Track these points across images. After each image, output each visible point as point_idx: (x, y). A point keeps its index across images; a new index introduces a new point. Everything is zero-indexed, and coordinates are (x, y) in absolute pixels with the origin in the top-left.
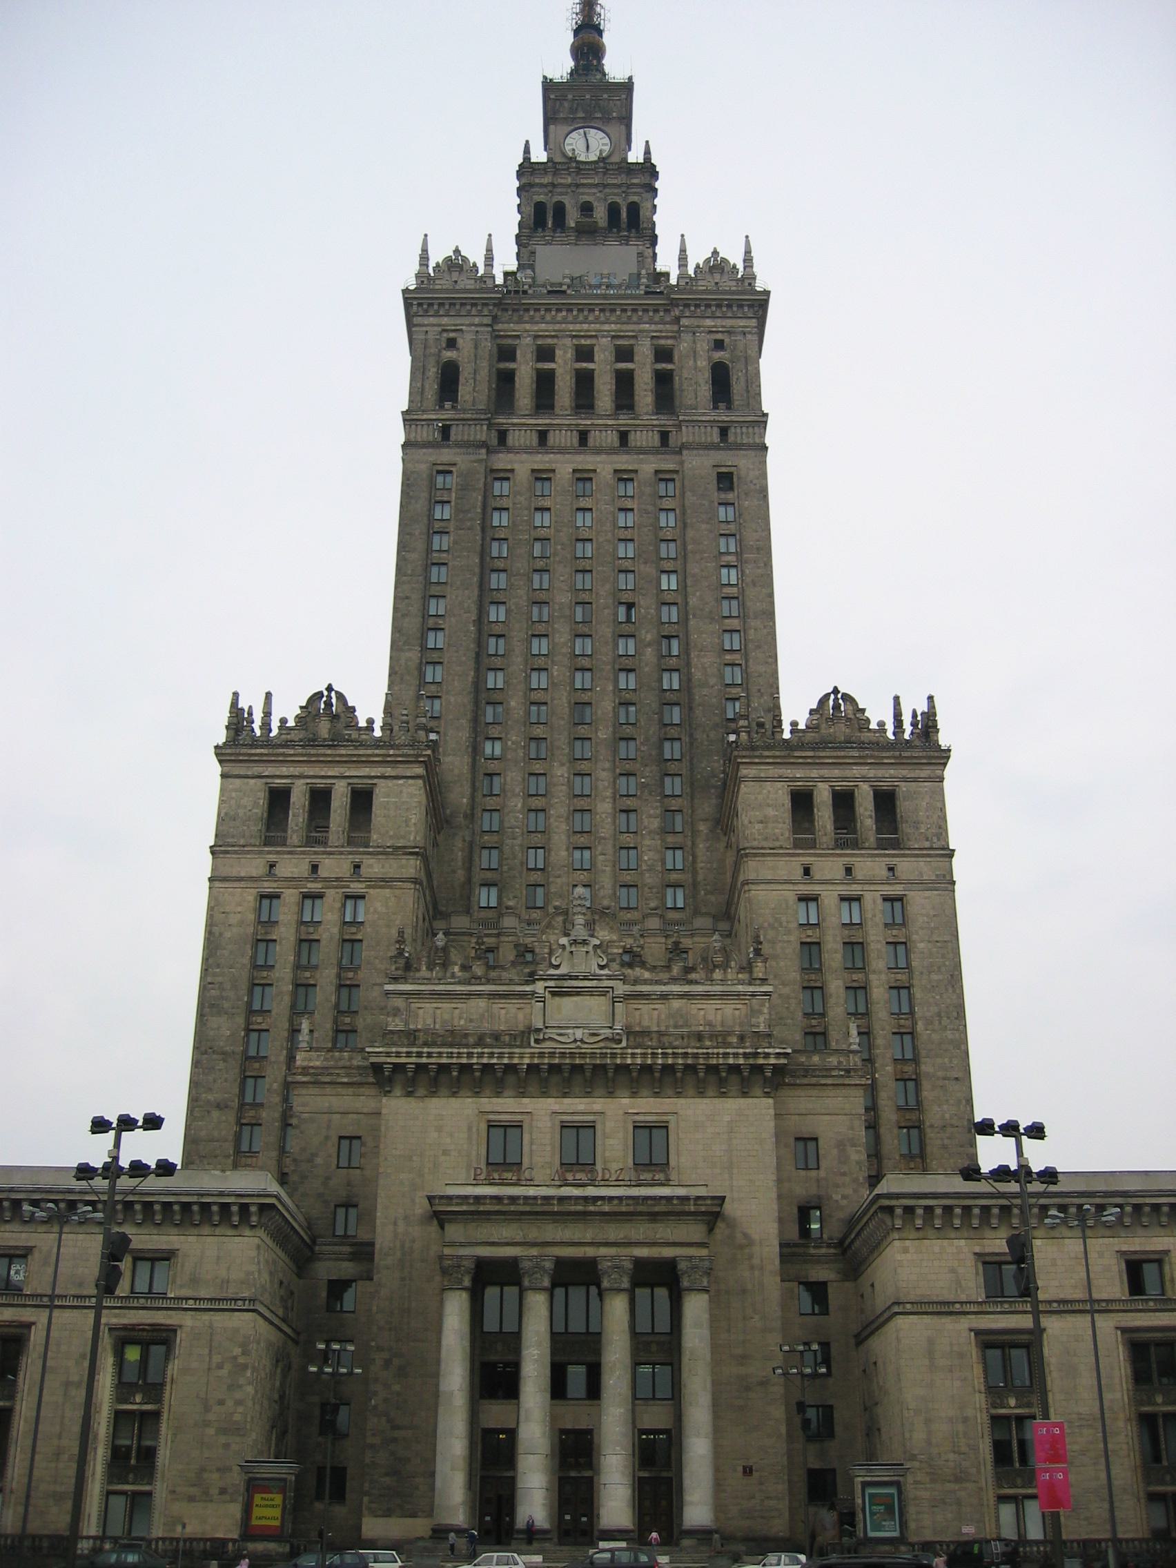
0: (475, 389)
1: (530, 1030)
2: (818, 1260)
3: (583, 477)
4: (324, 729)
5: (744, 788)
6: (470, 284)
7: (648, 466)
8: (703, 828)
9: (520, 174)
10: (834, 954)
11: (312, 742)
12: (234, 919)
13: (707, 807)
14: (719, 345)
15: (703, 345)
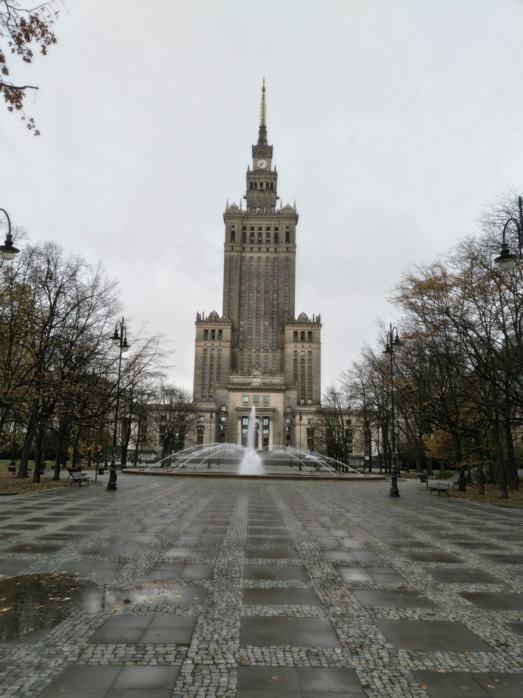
0: (238, 237)
2: (289, 415)
4: (214, 319)
6: (237, 212)
7: (272, 256)
8: (280, 332)
9: (247, 174)
11: (211, 321)
12: (200, 353)
13: (280, 328)
15: (284, 228)
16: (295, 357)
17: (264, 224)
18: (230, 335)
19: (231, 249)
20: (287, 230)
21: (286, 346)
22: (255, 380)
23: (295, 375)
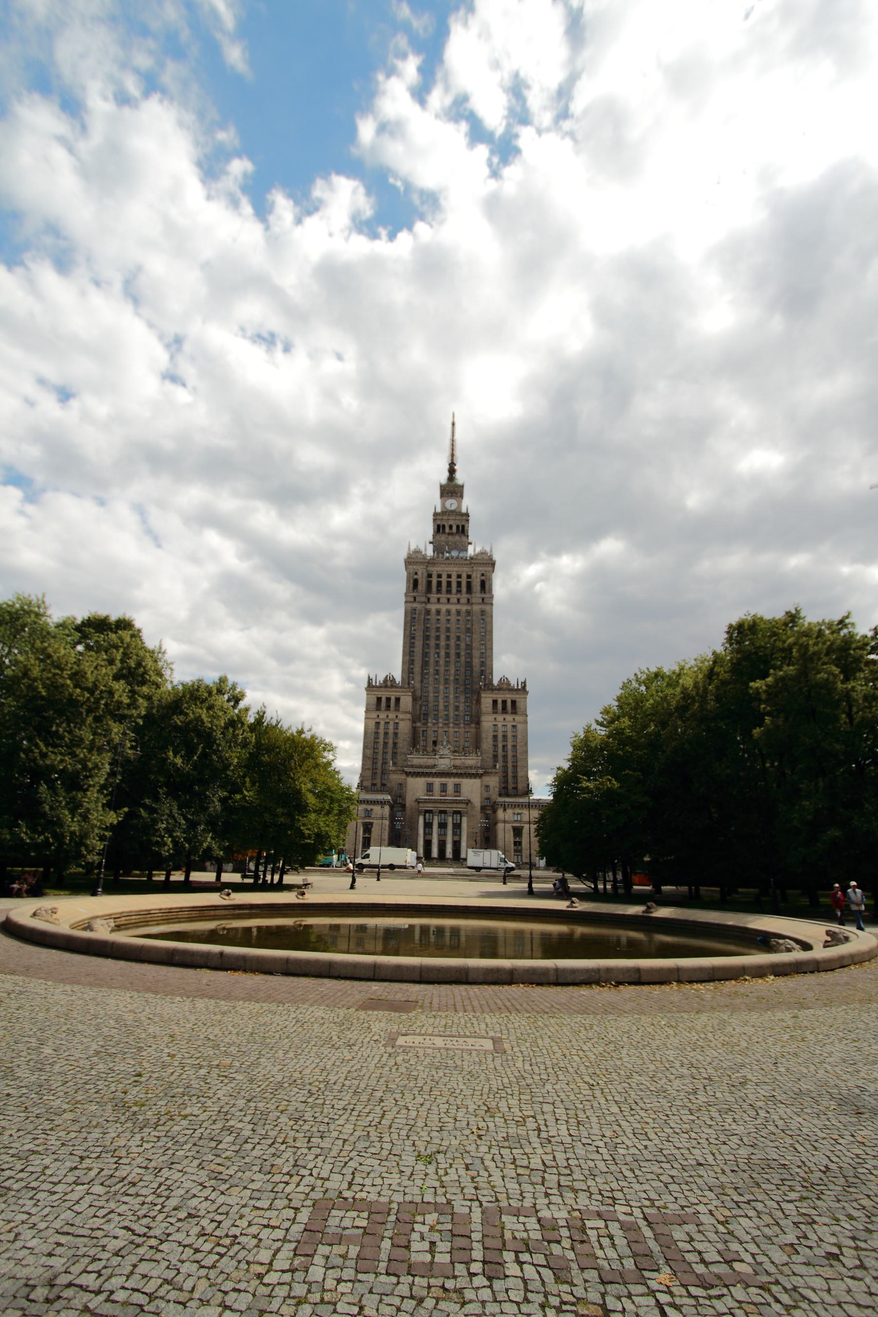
0: (422, 586)
3: (449, 612)
4: (389, 683)
5: (483, 700)
6: (420, 556)
7: (464, 608)
10: (500, 738)
11: (386, 686)
13: (475, 697)
14: (483, 575)
15: (479, 575)
16: (495, 734)
18: (410, 705)
19: (412, 600)
20: (483, 578)
21: (483, 718)
22: (442, 761)
23: (495, 757)
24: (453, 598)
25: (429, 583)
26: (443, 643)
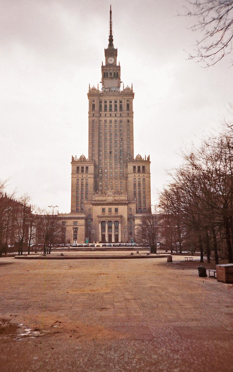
0: (97, 108)
1: (106, 200)
2: (131, 219)
4: (82, 160)
6: (95, 92)
7: (119, 119)
9: (102, 68)
10: (137, 185)
11: (81, 161)
13: (125, 165)
15: (126, 101)
16: (134, 183)
17: (113, 99)
18: (93, 170)
20: (128, 102)
21: (129, 176)
23: (135, 194)
24: (113, 114)
25: (100, 106)
26: (108, 138)
